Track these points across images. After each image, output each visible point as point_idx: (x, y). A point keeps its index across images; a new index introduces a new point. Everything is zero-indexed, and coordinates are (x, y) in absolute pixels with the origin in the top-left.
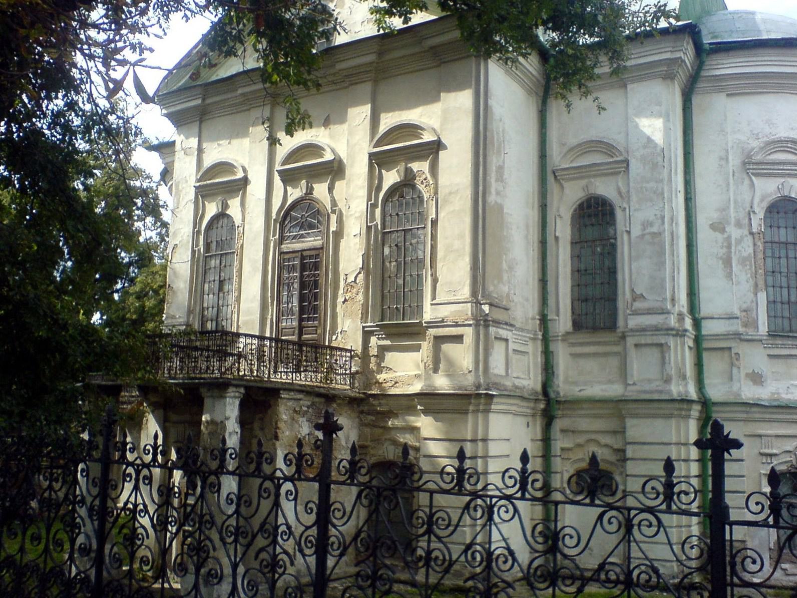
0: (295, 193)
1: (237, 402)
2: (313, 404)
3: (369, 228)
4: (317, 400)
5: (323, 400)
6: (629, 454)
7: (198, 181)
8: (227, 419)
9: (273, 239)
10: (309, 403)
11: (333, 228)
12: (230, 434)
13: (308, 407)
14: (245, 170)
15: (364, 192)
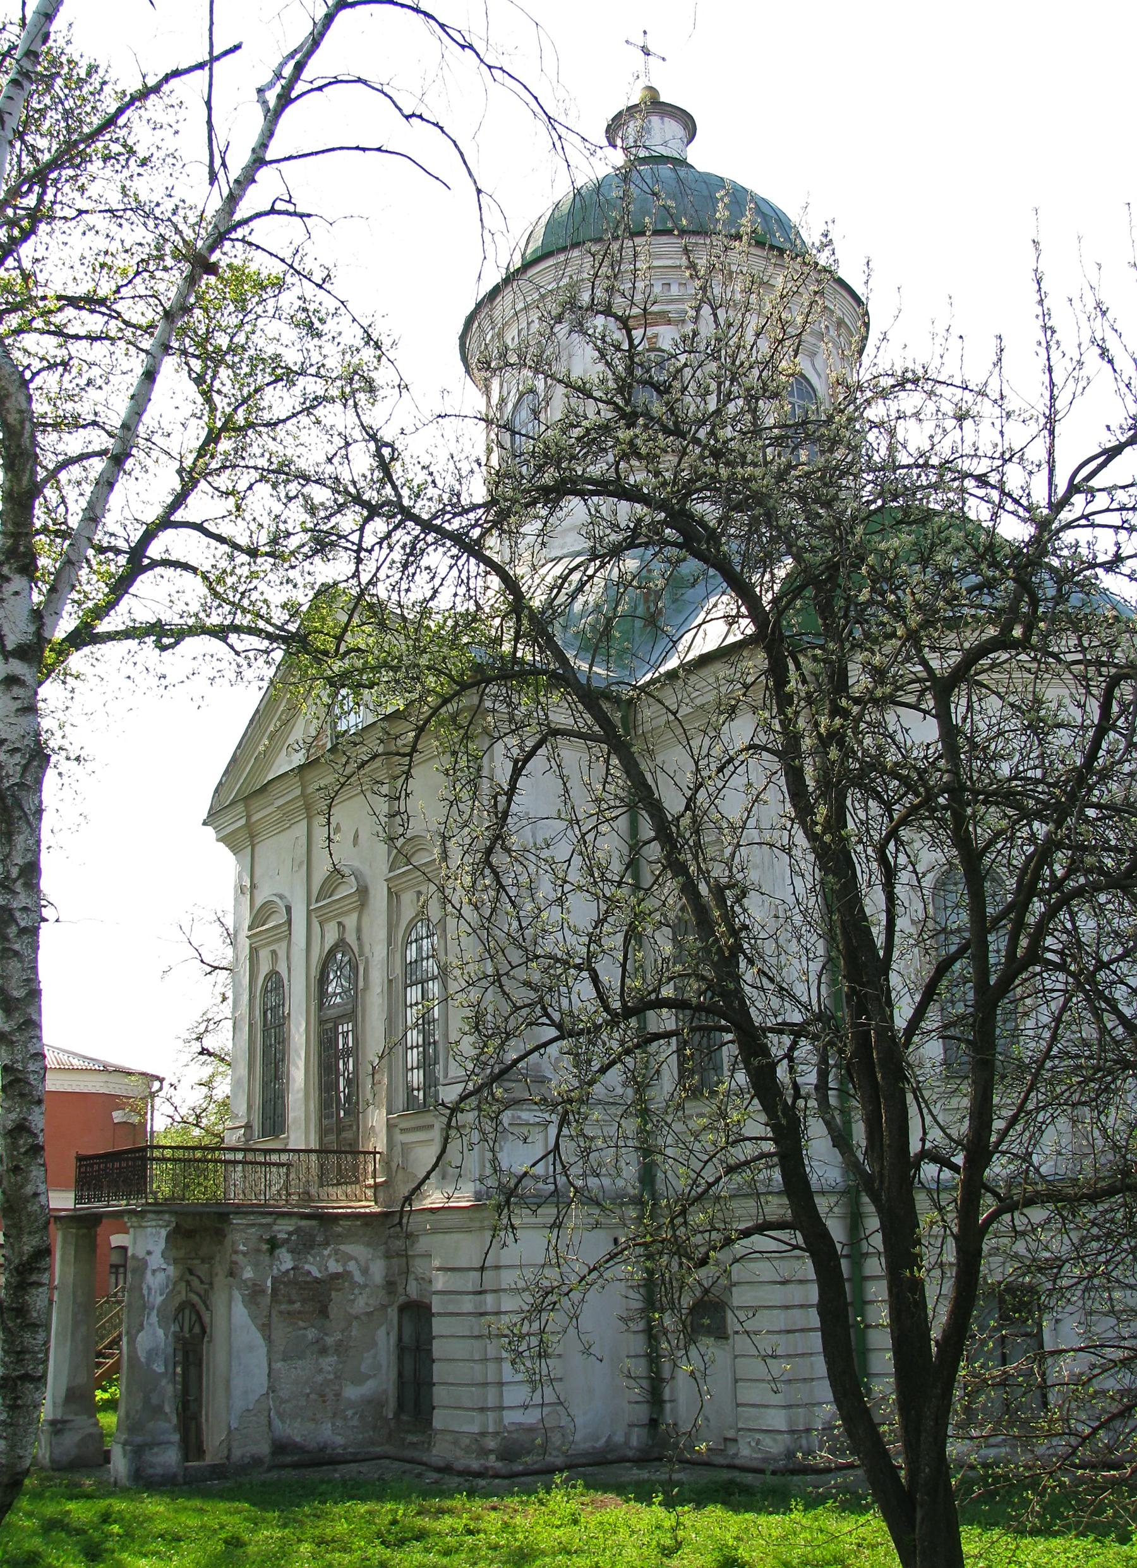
0: (331, 938)
1: (164, 1233)
2: (298, 1230)
3: (390, 981)
4: (304, 1223)
5: (314, 1223)
6: (735, 1278)
7: (250, 928)
8: (149, 1253)
9: (314, 1004)
10: (291, 1229)
11: (361, 984)
12: (154, 1271)
13: (290, 1234)
14: (289, 909)
15: (383, 934)
